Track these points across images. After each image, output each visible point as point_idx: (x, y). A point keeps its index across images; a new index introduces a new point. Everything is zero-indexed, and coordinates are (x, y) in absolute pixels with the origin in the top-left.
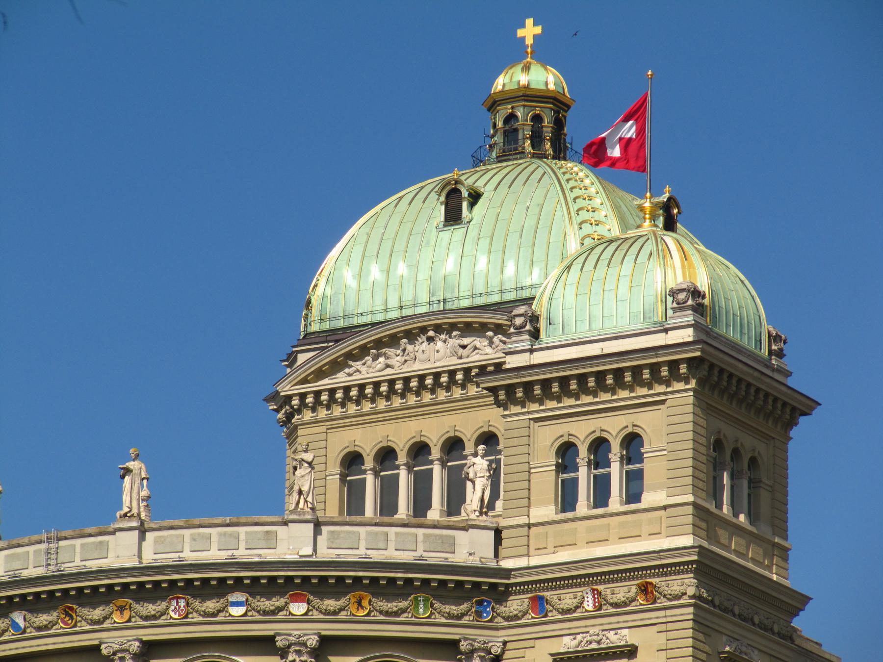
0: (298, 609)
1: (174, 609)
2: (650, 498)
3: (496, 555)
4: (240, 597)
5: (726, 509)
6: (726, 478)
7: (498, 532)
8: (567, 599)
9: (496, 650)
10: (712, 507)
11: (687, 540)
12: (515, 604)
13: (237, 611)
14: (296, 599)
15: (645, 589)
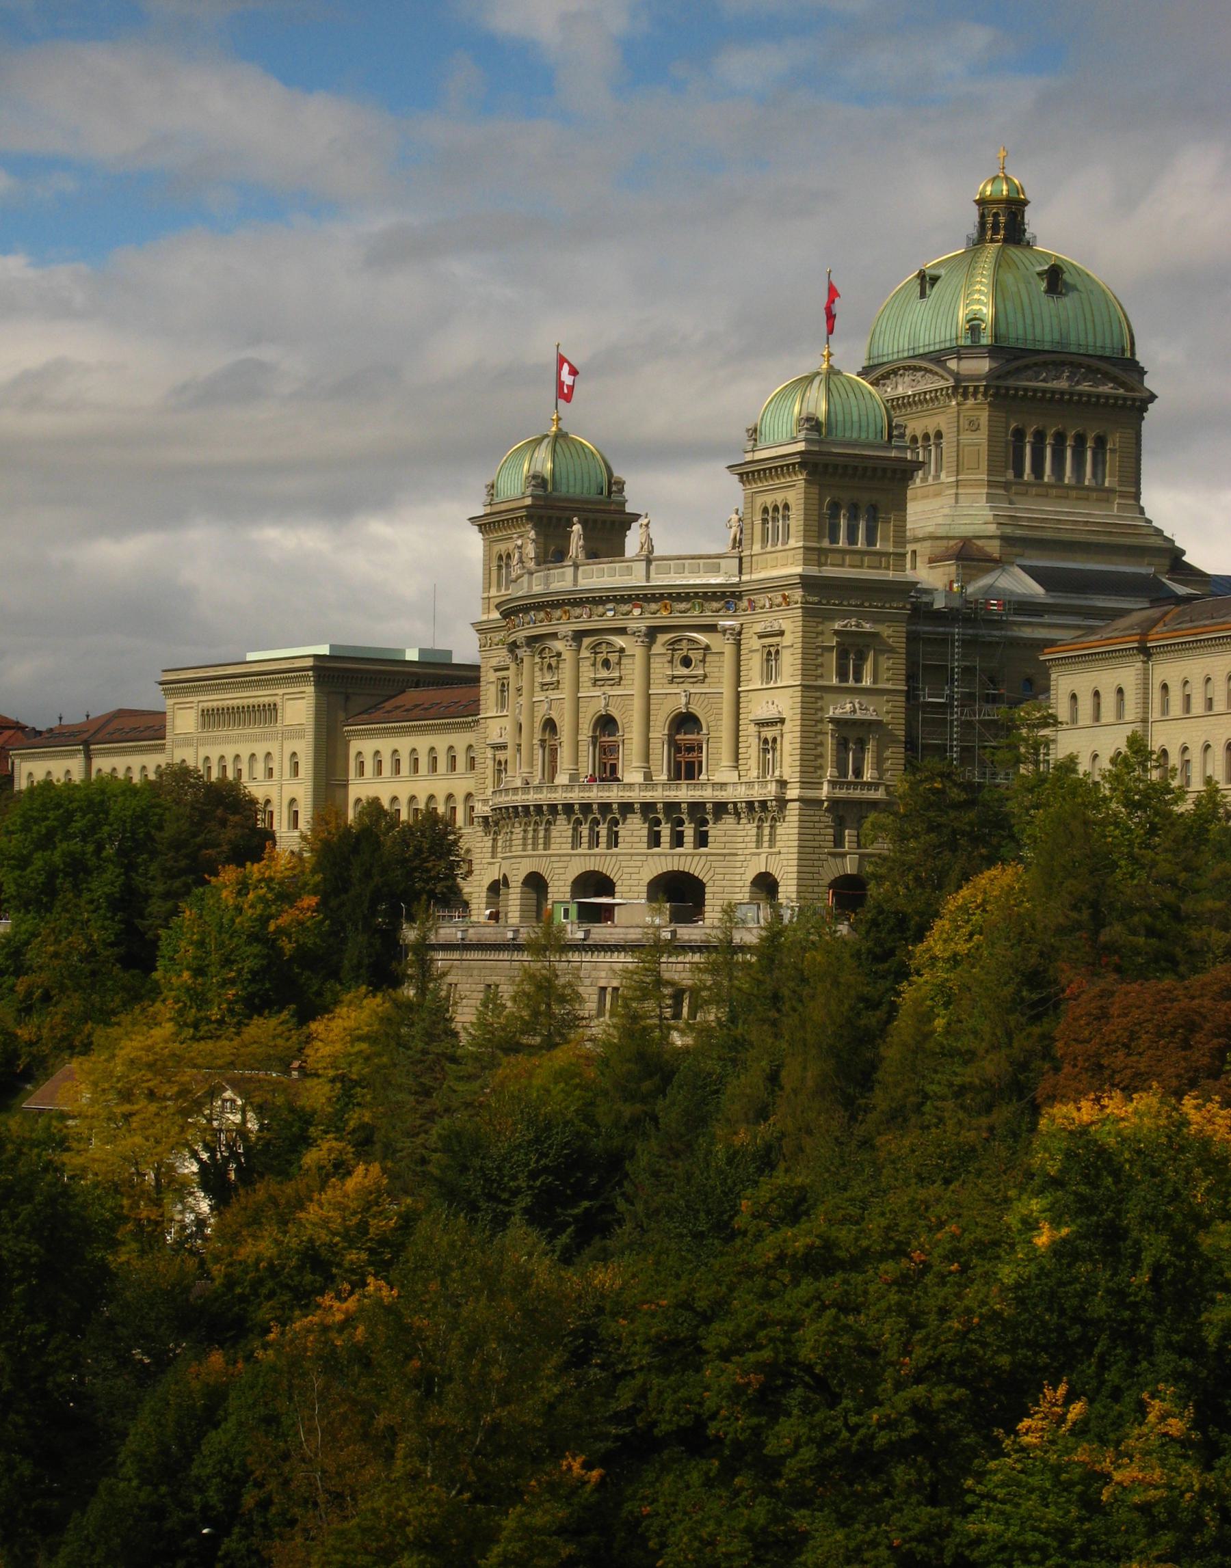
0: (637, 612)
1: (584, 612)
2: (793, 543)
3: (740, 572)
4: (610, 606)
5: (842, 543)
6: (843, 523)
7: (741, 559)
8: (762, 600)
9: (737, 629)
10: (826, 544)
11: (799, 570)
12: (744, 603)
13: (610, 614)
14: (636, 606)
15: (784, 597)
